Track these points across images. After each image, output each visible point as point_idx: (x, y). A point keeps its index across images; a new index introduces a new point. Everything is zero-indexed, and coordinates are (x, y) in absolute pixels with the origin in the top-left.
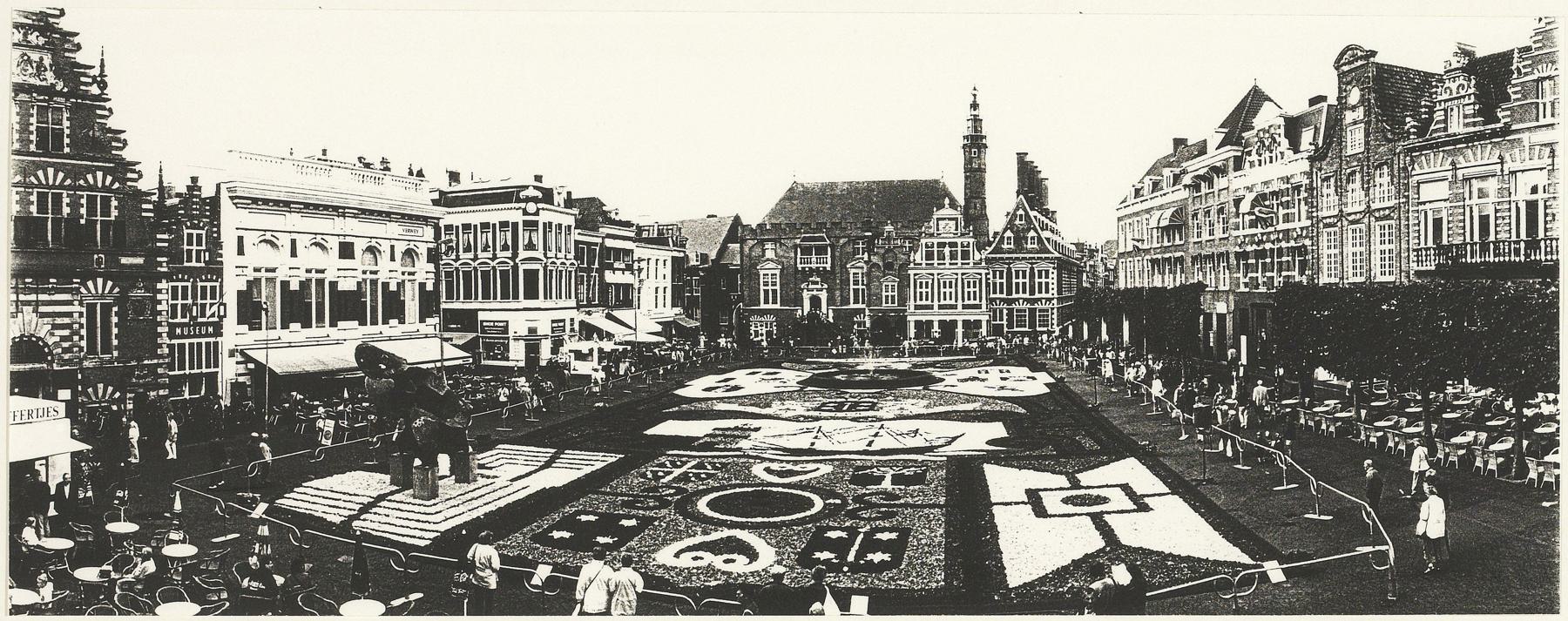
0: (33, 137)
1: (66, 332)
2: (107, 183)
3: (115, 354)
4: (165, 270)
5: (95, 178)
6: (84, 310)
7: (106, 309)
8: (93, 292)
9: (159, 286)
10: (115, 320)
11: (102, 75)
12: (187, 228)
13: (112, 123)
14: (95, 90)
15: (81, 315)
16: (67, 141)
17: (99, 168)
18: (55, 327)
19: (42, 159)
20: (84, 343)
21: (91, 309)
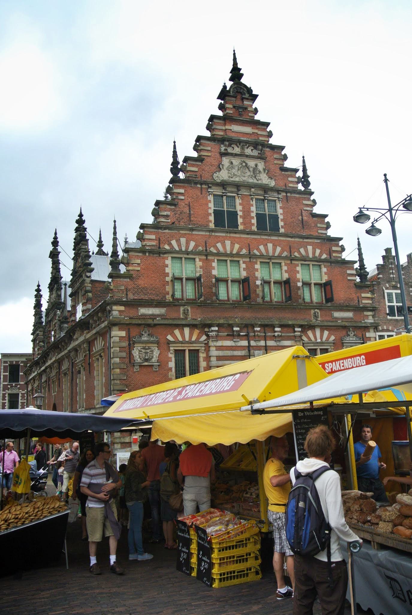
4: (372, 321)
5: (306, 251)
8: (313, 339)
9: (368, 335)
11: (306, 176)
12: (387, 288)
13: (317, 210)
14: (300, 187)
16: (281, 224)
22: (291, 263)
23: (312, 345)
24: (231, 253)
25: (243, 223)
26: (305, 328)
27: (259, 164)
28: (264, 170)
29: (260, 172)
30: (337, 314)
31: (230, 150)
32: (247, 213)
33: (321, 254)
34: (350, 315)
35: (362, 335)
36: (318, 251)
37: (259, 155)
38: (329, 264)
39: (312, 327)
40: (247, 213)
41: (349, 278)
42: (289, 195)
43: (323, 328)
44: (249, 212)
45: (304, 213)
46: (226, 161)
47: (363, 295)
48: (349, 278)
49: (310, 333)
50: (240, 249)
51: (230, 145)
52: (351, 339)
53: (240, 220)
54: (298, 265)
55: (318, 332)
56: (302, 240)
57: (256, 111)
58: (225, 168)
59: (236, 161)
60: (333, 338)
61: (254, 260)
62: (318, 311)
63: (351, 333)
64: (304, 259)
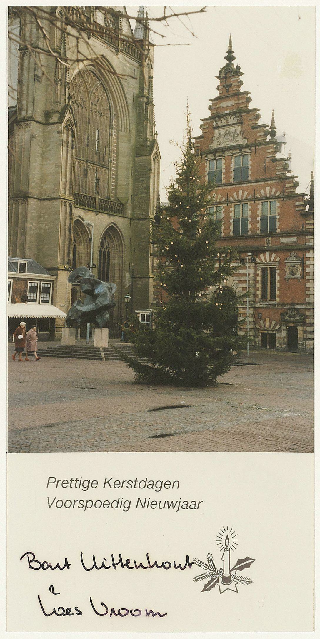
0: (232, 175)
1: (244, 285)
2: (273, 193)
3: (278, 300)
5: (265, 192)
6: (259, 272)
7: (273, 270)
8: (264, 261)
10: (278, 278)
11: (273, 128)
15: (256, 274)
16: (250, 172)
17: (267, 185)
18: (240, 282)
19: (237, 186)
20: (259, 293)
21: (264, 270)
22: (254, 202)
23: (263, 265)
24: (216, 202)
25: (225, 178)
26: (257, 252)
27: (238, 128)
28: (240, 132)
29: (238, 134)
30: (284, 240)
31: (220, 124)
32: (228, 168)
33: (275, 192)
34: (293, 239)
35: (303, 255)
36: (274, 190)
37: (239, 121)
38: (282, 199)
39: (264, 252)
40: (228, 168)
41: (297, 209)
42: (257, 148)
43: (271, 251)
44: (230, 168)
45: (267, 160)
46: (217, 132)
47: (307, 222)
48: (297, 209)
49: (262, 256)
50: (222, 198)
51: (219, 120)
52: (292, 259)
53: (223, 176)
54: (259, 204)
55: (268, 254)
56: (263, 183)
57: (241, 83)
58: (216, 138)
59: (223, 131)
60: (278, 259)
61: (230, 205)
62: (270, 239)
63: (293, 255)
64: (263, 198)
